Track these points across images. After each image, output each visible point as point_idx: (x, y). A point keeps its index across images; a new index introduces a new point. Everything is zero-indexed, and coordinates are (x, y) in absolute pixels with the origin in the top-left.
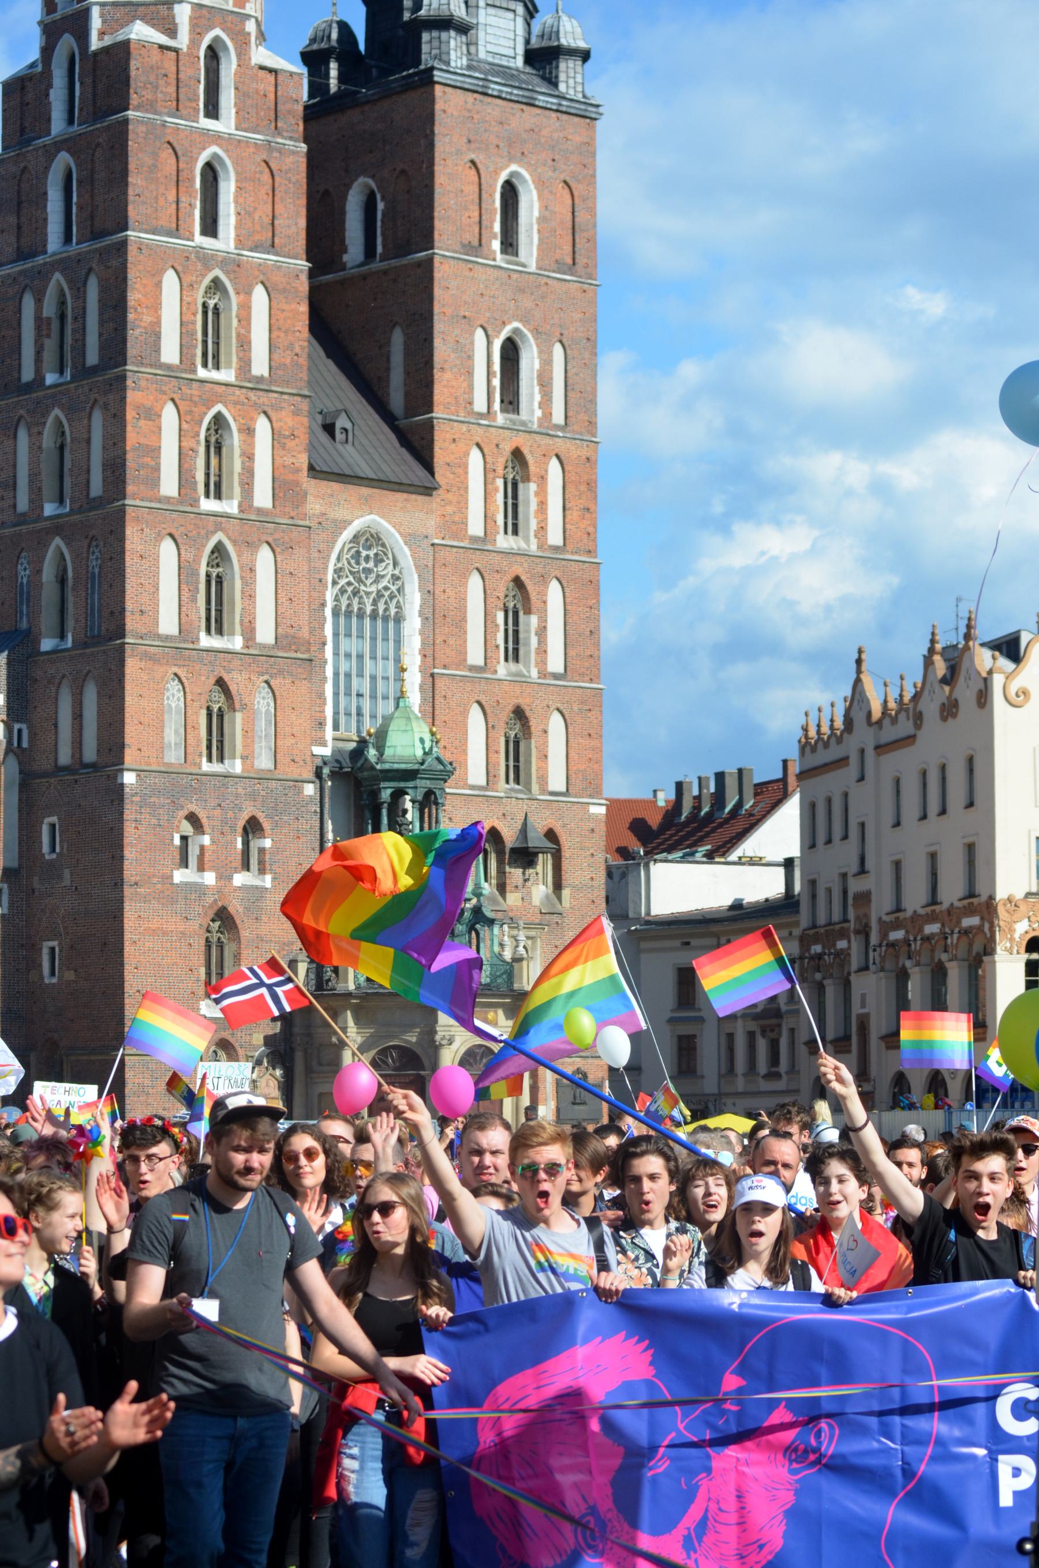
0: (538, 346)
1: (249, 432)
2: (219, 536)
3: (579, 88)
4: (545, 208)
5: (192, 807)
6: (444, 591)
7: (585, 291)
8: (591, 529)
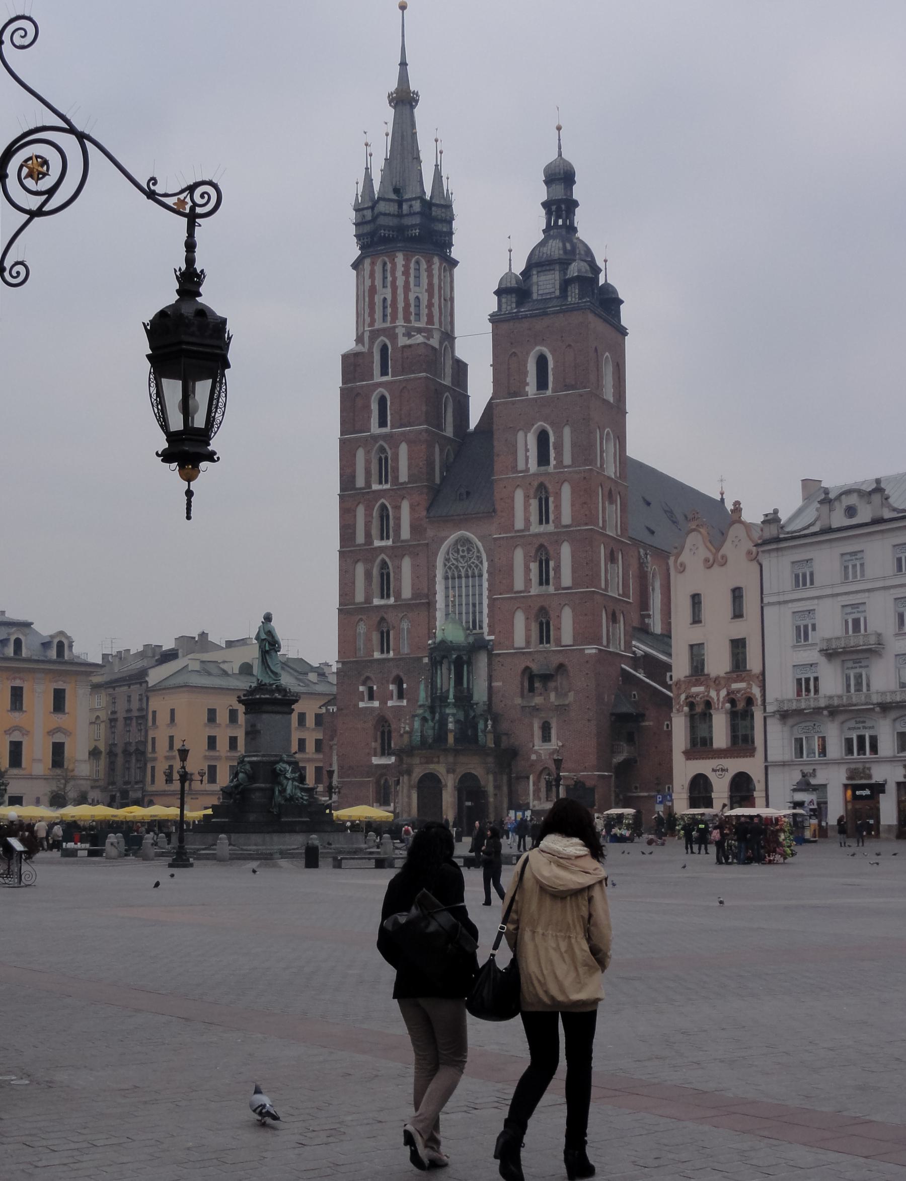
0: (553, 430)
1: (397, 508)
2: (383, 556)
3: (577, 296)
4: (556, 362)
5: (368, 674)
6: (500, 559)
7: (581, 396)
8: (587, 513)
